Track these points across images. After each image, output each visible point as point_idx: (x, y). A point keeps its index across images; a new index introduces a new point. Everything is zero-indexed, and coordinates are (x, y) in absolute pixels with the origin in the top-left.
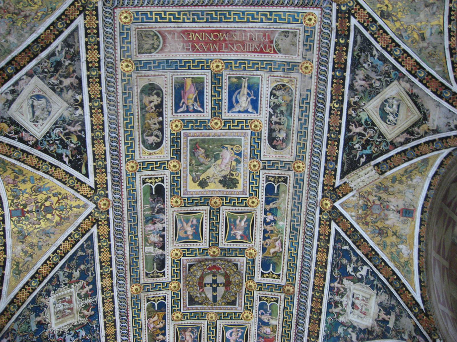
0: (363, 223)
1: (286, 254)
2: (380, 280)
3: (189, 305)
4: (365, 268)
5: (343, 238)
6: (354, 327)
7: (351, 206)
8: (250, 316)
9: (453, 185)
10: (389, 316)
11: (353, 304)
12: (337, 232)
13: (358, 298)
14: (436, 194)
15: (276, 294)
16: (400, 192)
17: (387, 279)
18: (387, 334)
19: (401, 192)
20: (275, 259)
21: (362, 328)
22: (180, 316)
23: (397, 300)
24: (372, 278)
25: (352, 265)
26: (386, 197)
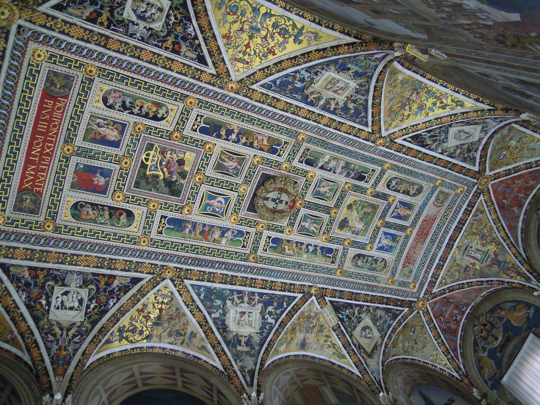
2: (269, 334)
4: (273, 321)
5: (291, 303)
6: (224, 314)
10: (245, 345)
11: (244, 313)
12: (295, 298)
13: (249, 317)
15: (250, 247)
16: (318, 340)
17: (271, 340)
18: (231, 346)
19: (318, 341)
20: (279, 249)
21: (226, 322)
24: (267, 327)
25: (273, 311)
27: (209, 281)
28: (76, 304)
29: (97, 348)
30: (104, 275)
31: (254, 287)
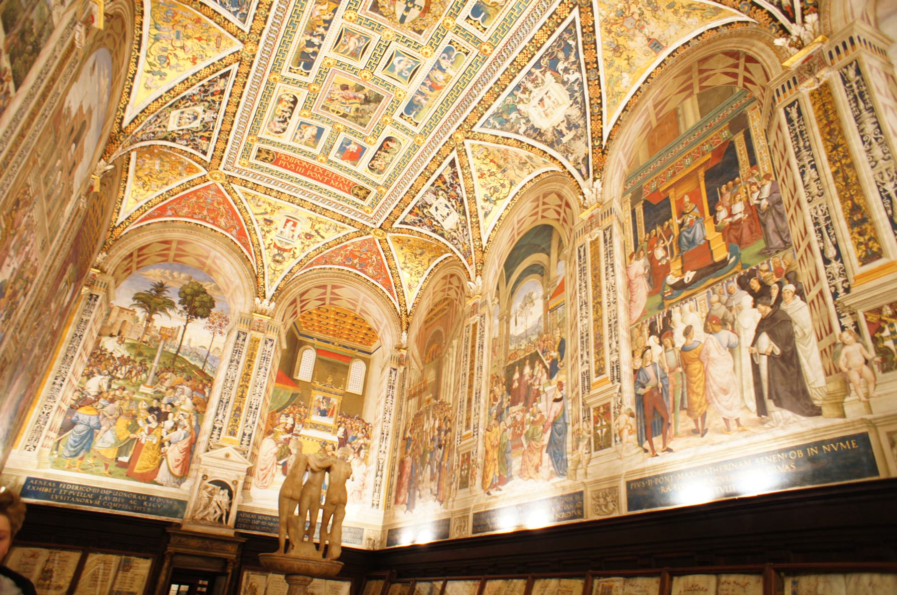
0: (606, 29)
1: (506, 12)
2: (583, 94)
3: (371, 10)
4: (577, 75)
6: (528, 121)
7: (607, 3)
8: (430, 53)
9: (721, 55)
11: (542, 100)
12: (573, 22)
13: (549, 97)
14: (698, 48)
17: (591, 99)
19: (667, 22)
20: (490, 10)
21: (536, 126)
22: (353, 18)
23: (586, 122)
24: (576, 88)
25: (566, 64)
26: (648, 17)
27: (487, 109)
28: (447, 210)
29: (481, 226)
30: (436, 180)
31: (523, 67)
